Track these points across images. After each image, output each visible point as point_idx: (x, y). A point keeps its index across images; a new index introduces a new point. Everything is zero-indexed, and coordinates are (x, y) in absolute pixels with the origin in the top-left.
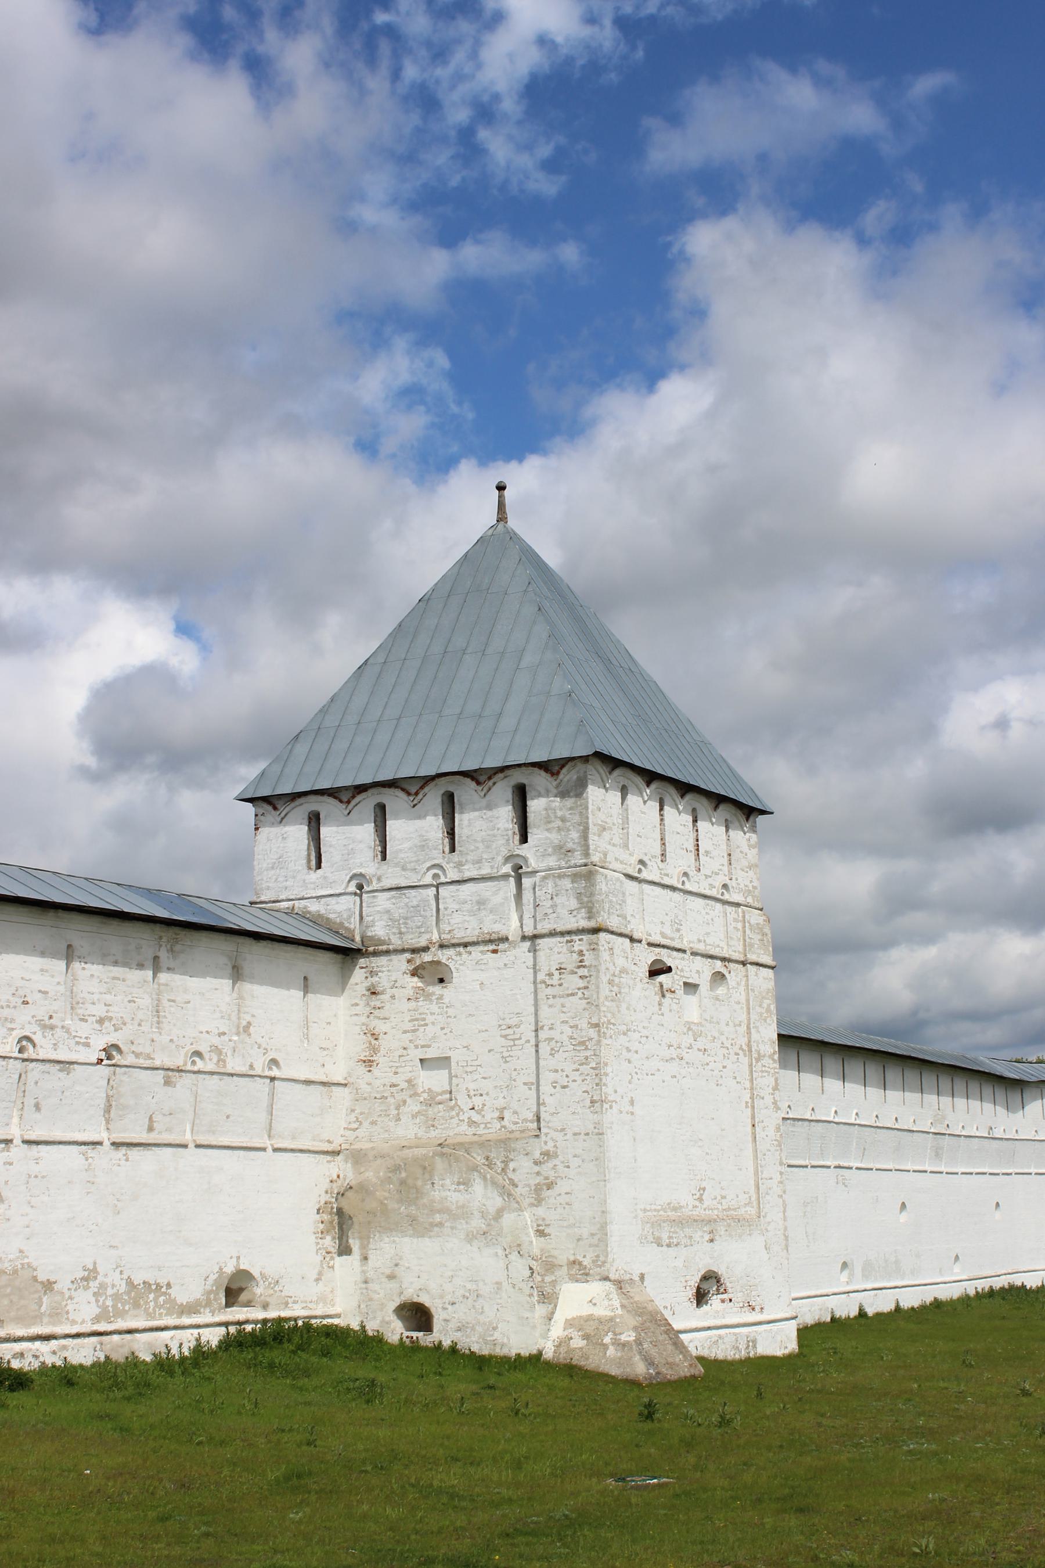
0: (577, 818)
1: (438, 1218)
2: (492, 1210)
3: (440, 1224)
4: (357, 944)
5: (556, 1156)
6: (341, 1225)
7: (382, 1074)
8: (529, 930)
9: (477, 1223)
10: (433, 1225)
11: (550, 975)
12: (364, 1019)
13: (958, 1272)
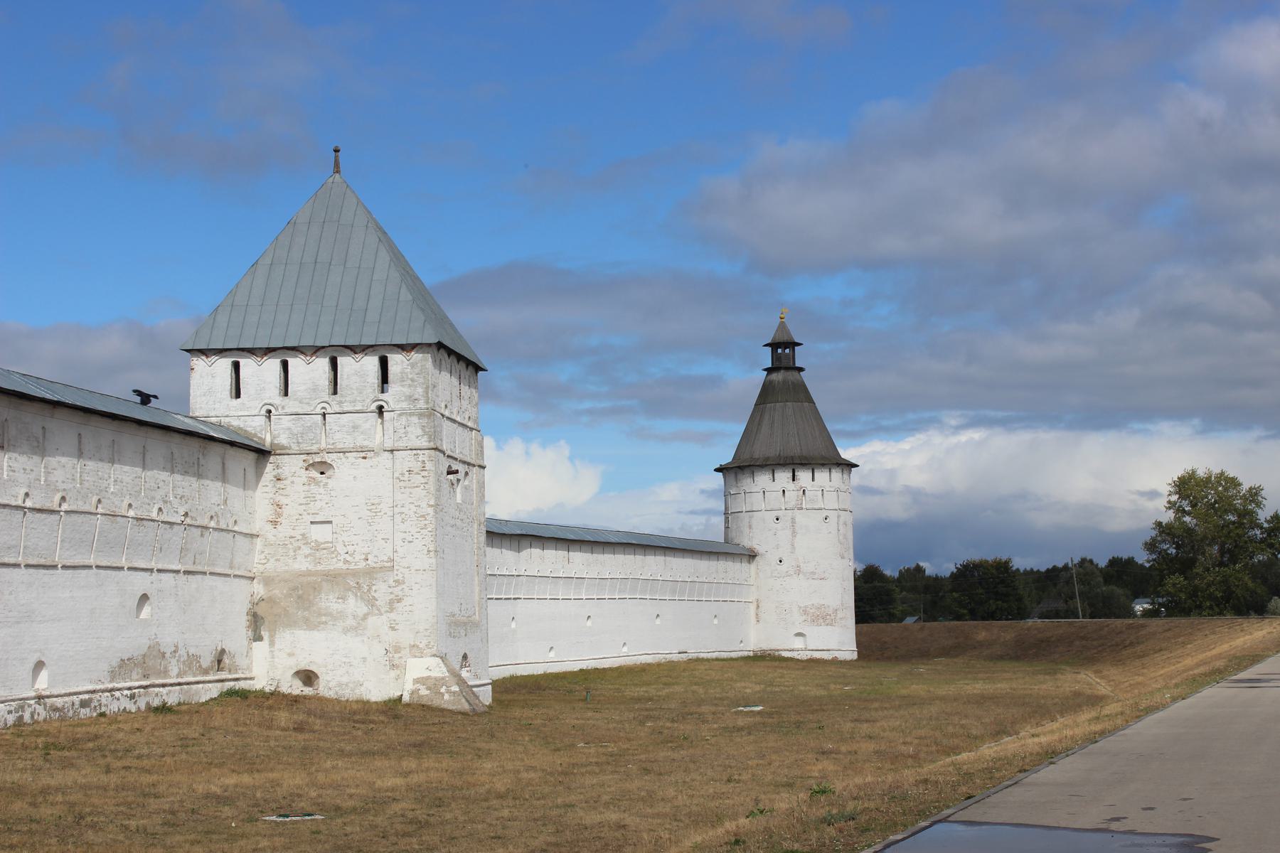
0: (422, 380)
1: (324, 619)
2: (361, 615)
3: (326, 623)
4: (267, 447)
5: (404, 583)
6: (256, 622)
7: (284, 530)
8: (389, 445)
9: (350, 622)
10: (320, 623)
11: (403, 474)
12: (271, 495)
13: (798, 643)
